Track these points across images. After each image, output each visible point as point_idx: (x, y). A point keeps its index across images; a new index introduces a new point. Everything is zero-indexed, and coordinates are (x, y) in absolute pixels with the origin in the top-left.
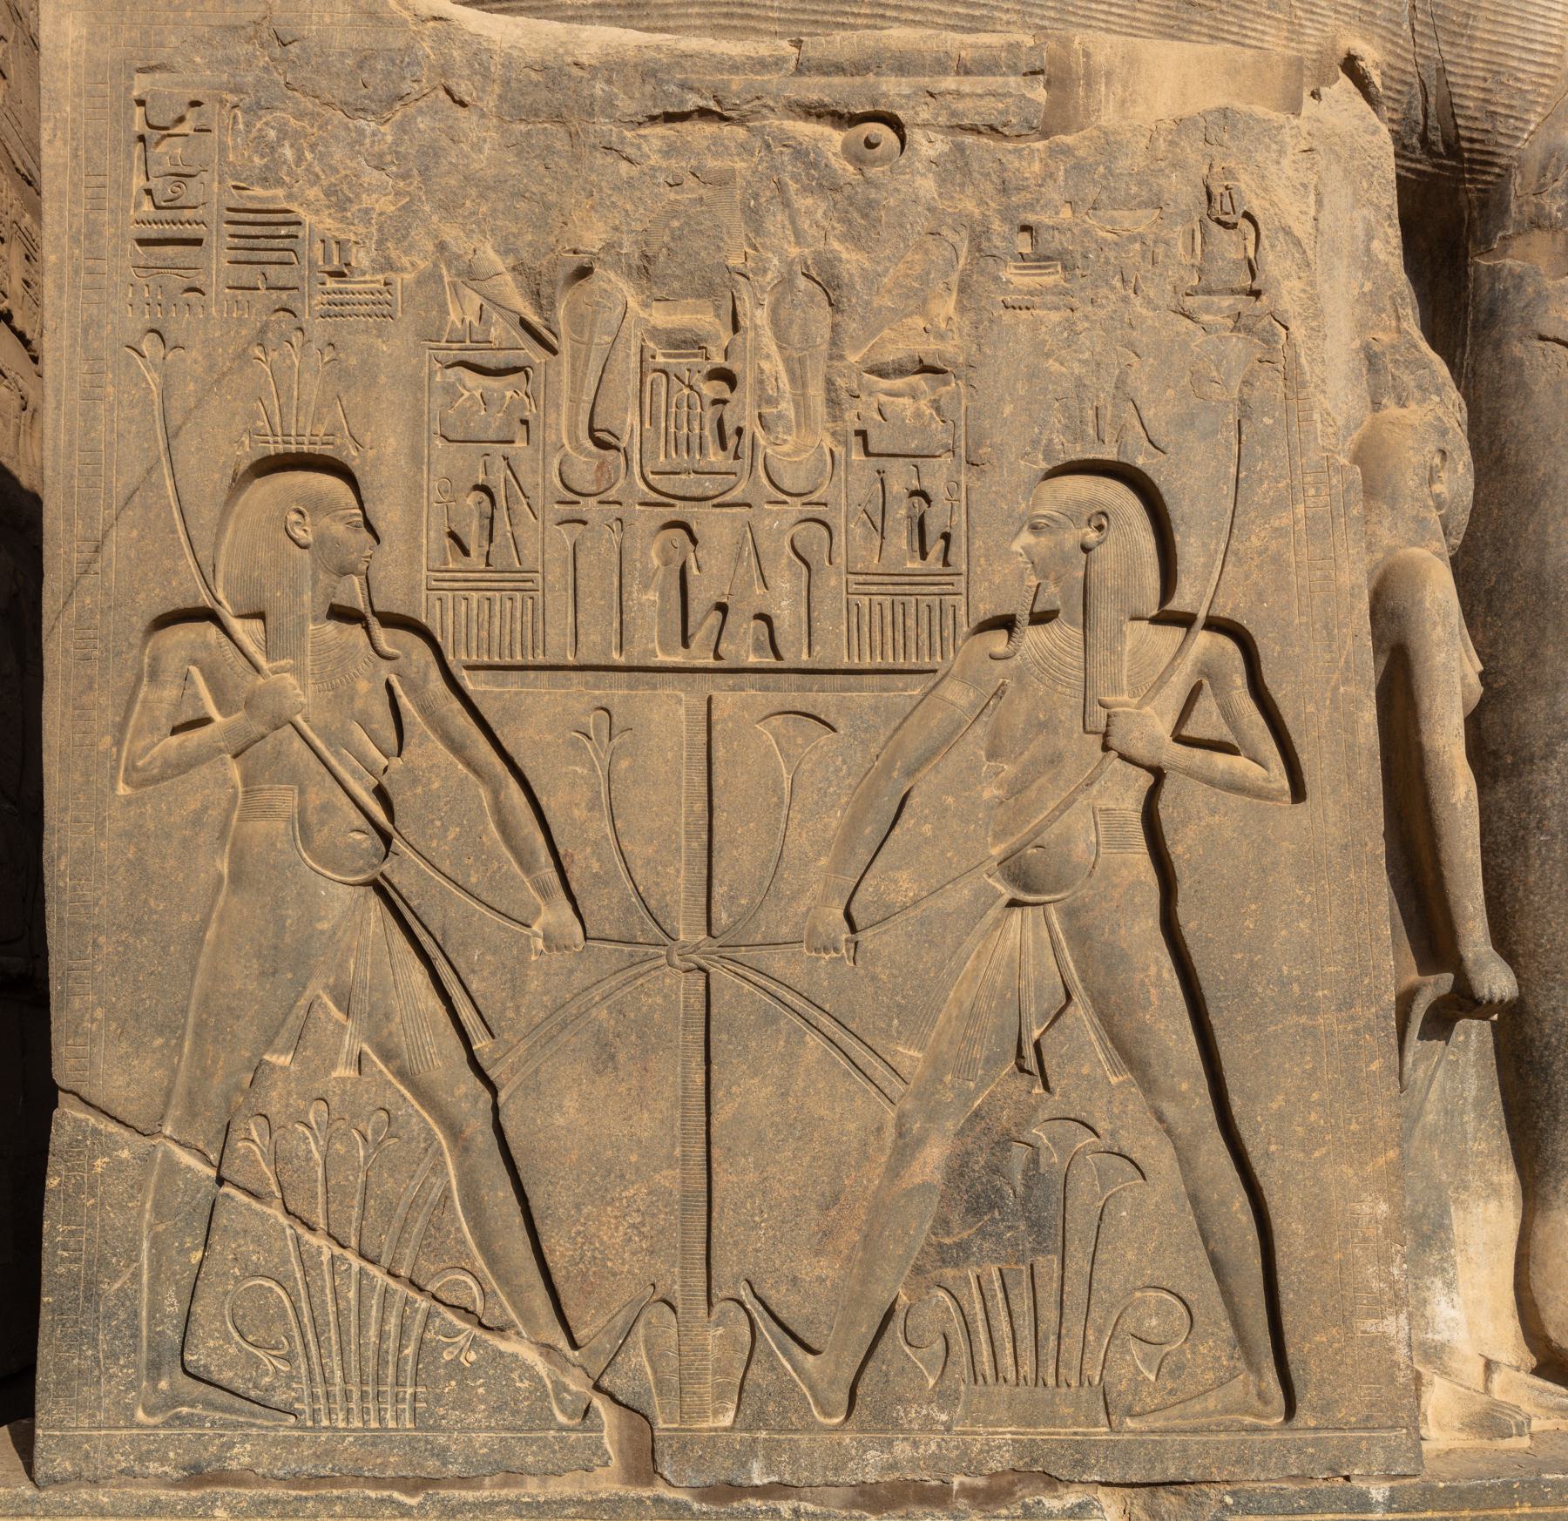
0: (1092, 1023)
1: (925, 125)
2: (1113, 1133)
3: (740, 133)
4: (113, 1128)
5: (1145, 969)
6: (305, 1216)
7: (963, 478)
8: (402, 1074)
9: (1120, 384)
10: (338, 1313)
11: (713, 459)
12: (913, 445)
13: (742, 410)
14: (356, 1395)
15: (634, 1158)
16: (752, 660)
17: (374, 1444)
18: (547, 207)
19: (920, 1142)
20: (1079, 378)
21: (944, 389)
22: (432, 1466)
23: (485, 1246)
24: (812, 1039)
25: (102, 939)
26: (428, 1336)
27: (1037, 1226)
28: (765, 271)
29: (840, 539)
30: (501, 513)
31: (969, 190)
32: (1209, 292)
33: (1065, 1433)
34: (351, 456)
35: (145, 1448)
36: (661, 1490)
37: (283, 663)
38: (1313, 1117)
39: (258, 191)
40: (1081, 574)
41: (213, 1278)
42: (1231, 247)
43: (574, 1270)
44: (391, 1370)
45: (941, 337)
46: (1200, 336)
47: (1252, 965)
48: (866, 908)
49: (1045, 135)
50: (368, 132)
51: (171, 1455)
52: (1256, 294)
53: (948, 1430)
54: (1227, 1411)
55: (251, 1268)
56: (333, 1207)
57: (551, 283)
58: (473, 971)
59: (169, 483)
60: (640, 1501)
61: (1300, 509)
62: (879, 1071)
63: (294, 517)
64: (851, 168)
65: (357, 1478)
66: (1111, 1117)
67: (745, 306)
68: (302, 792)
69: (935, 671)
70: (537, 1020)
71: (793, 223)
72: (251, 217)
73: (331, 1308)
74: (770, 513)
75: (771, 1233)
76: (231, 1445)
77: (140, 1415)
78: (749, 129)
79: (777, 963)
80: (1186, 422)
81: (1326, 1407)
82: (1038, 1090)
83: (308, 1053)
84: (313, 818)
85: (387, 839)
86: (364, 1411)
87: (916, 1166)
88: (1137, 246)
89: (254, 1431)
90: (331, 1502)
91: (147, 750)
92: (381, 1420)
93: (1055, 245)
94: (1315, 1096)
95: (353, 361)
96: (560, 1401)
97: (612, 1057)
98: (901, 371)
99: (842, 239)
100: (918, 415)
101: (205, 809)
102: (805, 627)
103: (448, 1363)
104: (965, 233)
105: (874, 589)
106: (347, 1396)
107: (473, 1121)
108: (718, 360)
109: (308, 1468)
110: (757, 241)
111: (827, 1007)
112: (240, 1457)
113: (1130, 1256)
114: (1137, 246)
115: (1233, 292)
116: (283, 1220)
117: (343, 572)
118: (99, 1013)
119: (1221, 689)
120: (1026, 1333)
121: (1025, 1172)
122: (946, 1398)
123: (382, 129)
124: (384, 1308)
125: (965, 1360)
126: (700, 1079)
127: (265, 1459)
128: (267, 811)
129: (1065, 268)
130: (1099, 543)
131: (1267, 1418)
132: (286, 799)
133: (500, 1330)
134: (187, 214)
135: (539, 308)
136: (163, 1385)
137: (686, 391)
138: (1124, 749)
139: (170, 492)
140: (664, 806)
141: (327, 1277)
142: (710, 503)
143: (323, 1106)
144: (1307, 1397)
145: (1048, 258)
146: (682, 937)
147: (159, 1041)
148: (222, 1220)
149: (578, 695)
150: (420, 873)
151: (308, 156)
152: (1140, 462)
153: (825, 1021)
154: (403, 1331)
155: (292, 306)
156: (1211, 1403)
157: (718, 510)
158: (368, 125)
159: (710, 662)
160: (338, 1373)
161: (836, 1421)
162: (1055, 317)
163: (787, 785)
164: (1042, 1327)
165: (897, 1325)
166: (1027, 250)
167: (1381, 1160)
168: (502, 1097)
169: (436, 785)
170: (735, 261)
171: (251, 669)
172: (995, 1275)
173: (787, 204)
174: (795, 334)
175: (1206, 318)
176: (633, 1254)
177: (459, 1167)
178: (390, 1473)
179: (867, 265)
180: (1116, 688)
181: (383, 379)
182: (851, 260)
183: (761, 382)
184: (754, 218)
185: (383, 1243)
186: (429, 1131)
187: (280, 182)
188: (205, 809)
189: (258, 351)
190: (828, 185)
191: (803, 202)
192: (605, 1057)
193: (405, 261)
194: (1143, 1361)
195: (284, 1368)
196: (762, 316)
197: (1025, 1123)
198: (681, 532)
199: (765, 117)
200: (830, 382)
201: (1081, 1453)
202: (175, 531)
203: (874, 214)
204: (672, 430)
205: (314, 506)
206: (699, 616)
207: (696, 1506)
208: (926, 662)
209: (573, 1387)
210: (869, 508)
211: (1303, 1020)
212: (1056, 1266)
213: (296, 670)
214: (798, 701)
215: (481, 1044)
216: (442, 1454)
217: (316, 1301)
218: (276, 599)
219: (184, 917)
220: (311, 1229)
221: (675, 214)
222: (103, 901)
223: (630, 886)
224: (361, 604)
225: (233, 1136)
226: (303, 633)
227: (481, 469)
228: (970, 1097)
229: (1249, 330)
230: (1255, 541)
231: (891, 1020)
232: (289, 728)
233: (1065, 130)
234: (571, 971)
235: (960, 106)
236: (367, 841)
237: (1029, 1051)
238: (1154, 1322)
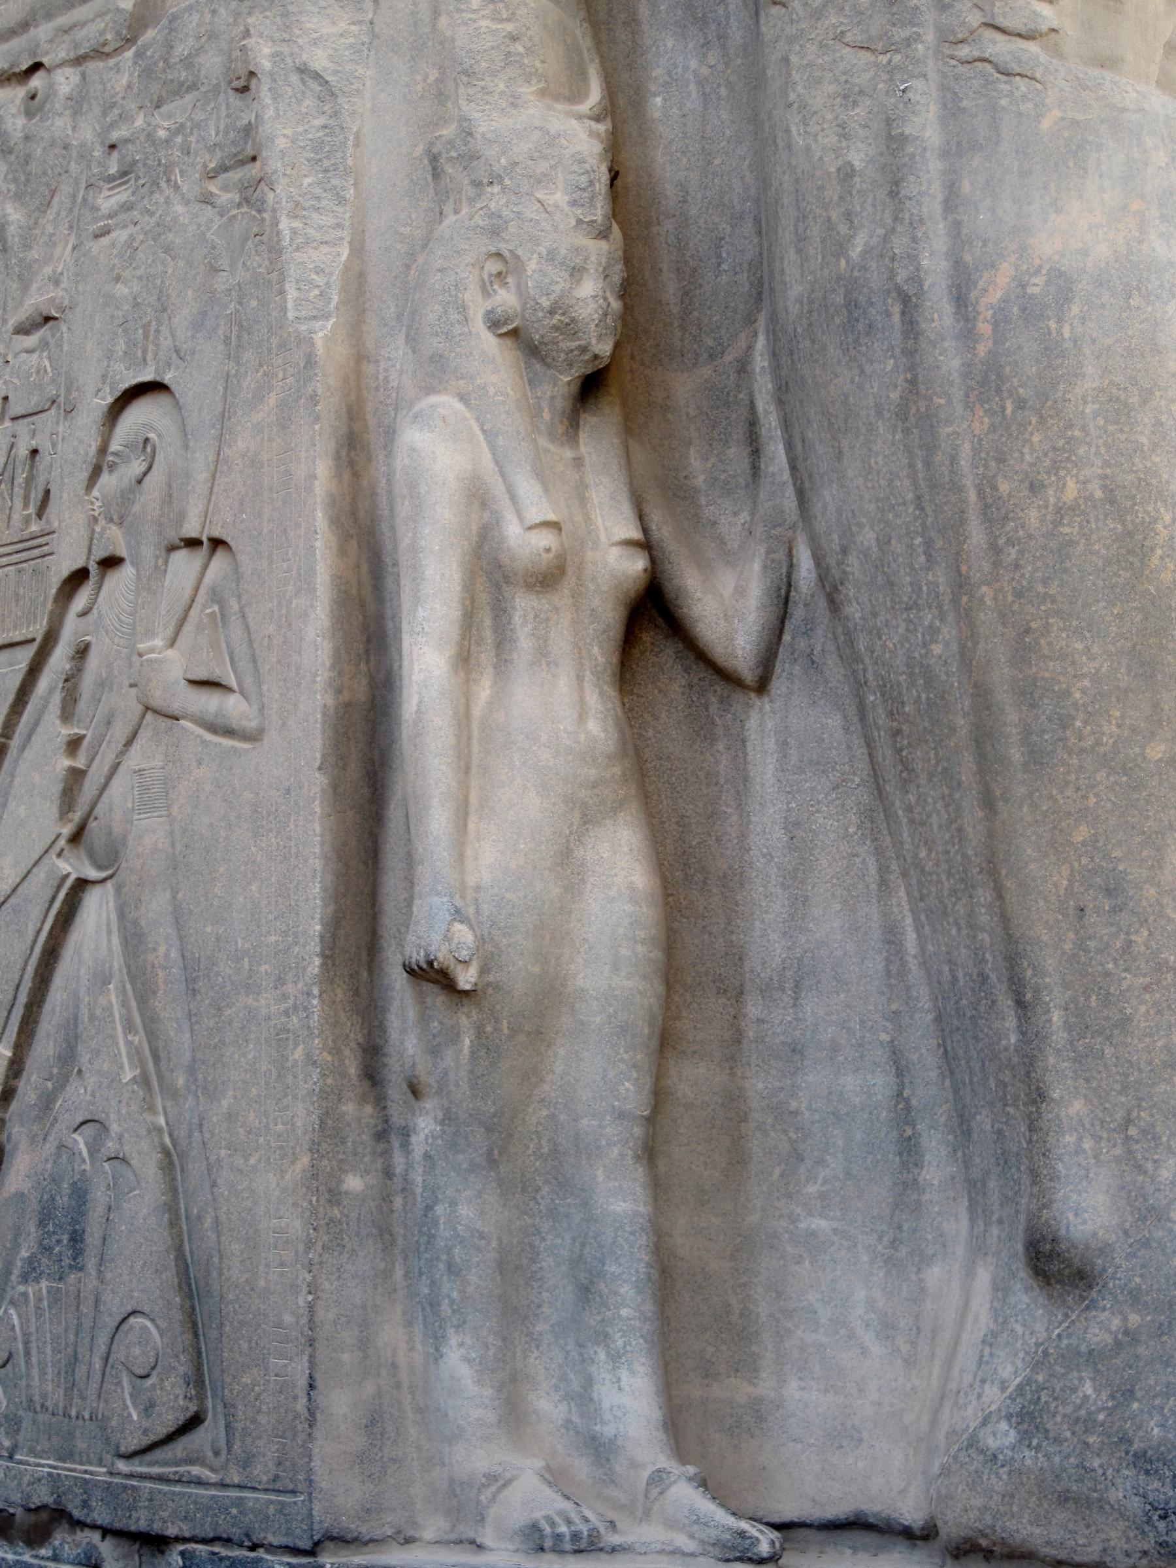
5: (154, 950)
61: (272, 400)
69: (33, 640)
81: (246, 1462)
115: (242, 163)
194: (131, 1395)
230: (241, 444)
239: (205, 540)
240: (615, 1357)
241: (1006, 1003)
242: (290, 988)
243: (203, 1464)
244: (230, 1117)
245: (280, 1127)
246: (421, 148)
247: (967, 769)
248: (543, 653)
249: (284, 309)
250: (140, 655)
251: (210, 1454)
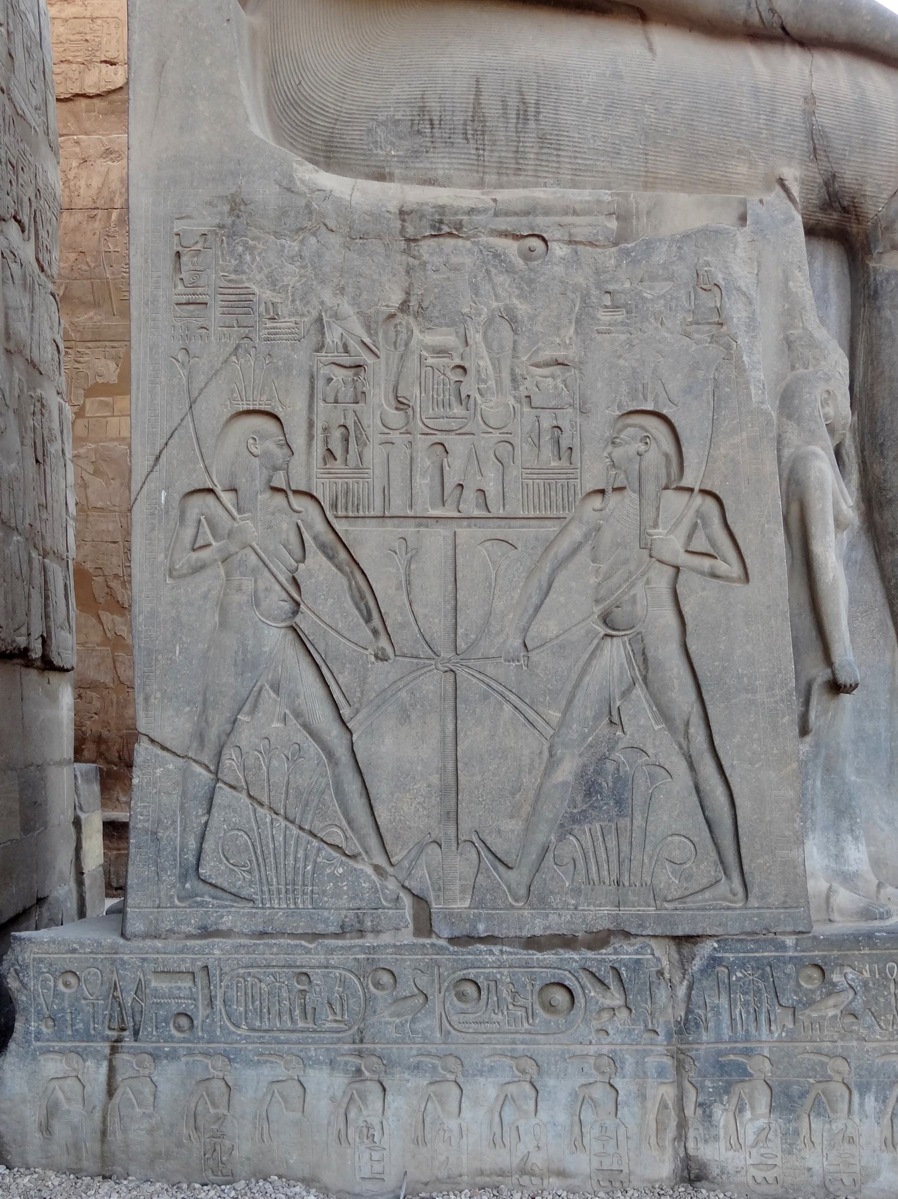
0: (645, 698)
1: (557, 241)
2: (656, 755)
3: (468, 244)
4: (165, 753)
6: (259, 798)
7: (578, 420)
8: (306, 726)
9: (655, 371)
10: (274, 849)
11: (455, 411)
12: (553, 403)
13: (469, 387)
14: (283, 891)
15: (419, 768)
16: (476, 513)
17: (293, 916)
18: (373, 281)
19: (561, 760)
20: (633, 368)
21: (568, 374)
22: (321, 928)
23: (346, 814)
24: (507, 707)
25: (160, 657)
26: (319, 860)
27: (619, 803)
28: (480, 315)
29: (518, 452)
30: (352, 439)
31: (580, 272)
32: (698, 324)
33: (633, 910)
34: (279, 411)
35: (179, 918)
36: (434, 940)
37: (246, 515)
38: (755, 746)
39: (233, 276)
40: (637, 467)
41: (214, 830)
42: (710, 301)
43: (390, 826)
44: (300, 877)
45: (567, 347)
46: (694, 347)
47: (724, 668)
48: (533, 639)
49: (616, 244)
50: (287, 246)
51: (193, 921)
52: (722, 324)
53: (576, 909)
54: (715, 899)
55: (232, 825)
56: (272, 794)
57: (376, 322)
58: (340, 673)
59: (191, 425)
60: (424, 945)
61: (744, 434)
62: (540, 723)
63: (251, 441)
64: (521, 262)
65: (283, 934)
66: (655, 746)
67: (471, 333)
68: (256, 581)
70: (371, 698)
71: (493, 288)
72: (231, 291)
73: (271, 846)
74: (483, 438)
75: (487, 806)
76: (222, 917)
77: (177, 902)
78: (473, 243)
79: (490, 670)
80: (688, 390)
81: (763, 896)
82: (619, 733)
83: (260, 715)
84: (261, 595)
85: (298, 604)
86: (287, 899)
87: (559, 772)
88: (662, 301)
89: (233, 909)
90: (271, 946)
91: (180, 560)
92: (295, 903)
93: (622, 301)
94: (756, 736)
95: (280, 363)
96: (384, 894)
97: (408, 717)
98: (547, 365)
99: (519, 297)
100: (556, 387)
101: (209, 591)
102: (501, 496)
103: (328, 874)
104: (578, 294)
105: (535, 476)
106: (279, 892)
107: (340, 749)
108: (458, 361)
109: (261, 928)
110: (476, 300)
111: (514, 691)
112: (227, 922)
113: (665, 818)
114: (662, 301)
115: (710, 323)
116: (248, 801)
117: (276, 469)
118: (158, 695)
119: (705, 525)
120: (614, 858)
121: (613, 775)
122: (576, 891)
123: (293, 244)
124: (297, 846)
125: (584, 872)
126: (451, 727)
127: (239, 924)
128: (239, 589)
129: (627, 312)
130: (646, 452)
131: (735, 902)
132: (248, 584)
133: (353, 857)
134: (200, 290)
135: (370, 335)
136: (188, 885)
137: (442, 377)
138: (659, 557)
139: (192, 430)
140: (432, 591)
141: (269, 829)
142: (454, 433)
143: (266, 741)
144: (755, 891)
145: (618, 307)
146: (442, 655)
147: (187, 709)
148: (217, 800)
149: (391, 530)
150: (314, 622)
151: (258, 258)
152: (665, 411)
153: (513, 697)
154: (306, 858)
155: (251, 336)
156: (707, 894)
157: (458, 437)
158: (287, 242)
159: (457, 515)
160: (275, 879)
161: (521, 904)
162: (623, 337)
163: (493, 576)
164: (622, 855)
165: (550, 855)
166: (609, 303)
167: (789, 768)
168: (354, 738)
169: (321, 578)
170: (466, 310)
171: (230, 518)
172: (598, 828)
173: (491, 280)
174: (495, 346)
175: (696, 336)
176: (419, 818)
177: (333, 772)
178: (300, 931)
179: (529, 311)
180: (655, 526)
181: (294, 372)
182: (522, 308)
183: (479, 371)
184: (476, 289)
185: (295, 812)
186: (319, 754)
187: (244, 272)
188: (209, 591)
189: (234, 358)
190: (510, 270)
192: (404, 716)
193: (305, 310)
194: (672, 873)
195: (248, 877)
196: (479, 337)
197: (611, 749)
198: (440, 447)
199: (479, 236)
200: (512, 370)
201: (642, 919)
202: (194, 450)
203: (533, 286)
204: (435, 396)
206: (449, 491)
207: (451, 948)
208: (561, 514)
209: (390, 887)
210: (533, 435)
211: (750, 696)
212: (629, 824)
213: (253, 519)
214: (499, 533)
215: (345, 711)
216: (325, 921)
217: (264, 842)
218: (242, 482)
219: (200, 646)
220: (261, 804)
221: (436, 286)
222: (160, 638)
223: (417, 628)
224: (285, 488)
225: (223, 757)
226: (256, 500)
227: (342, 417)
228: (585, 737)
229: (716, 342)
230: (722, 451)
231: (546, 696)
232: (248, 550)
233: (626, 241)
234: (388, 673)
235: (574, 231)
236: (287, 606)
237: (615, 712)
238: (677, 852)
239: (697, 489)
242: (777, 691)
243: (725, 899)
245: (775, 751)
246: (782, 336)
249: (749, 395)
250: (650, 535)
251: (730, 896)
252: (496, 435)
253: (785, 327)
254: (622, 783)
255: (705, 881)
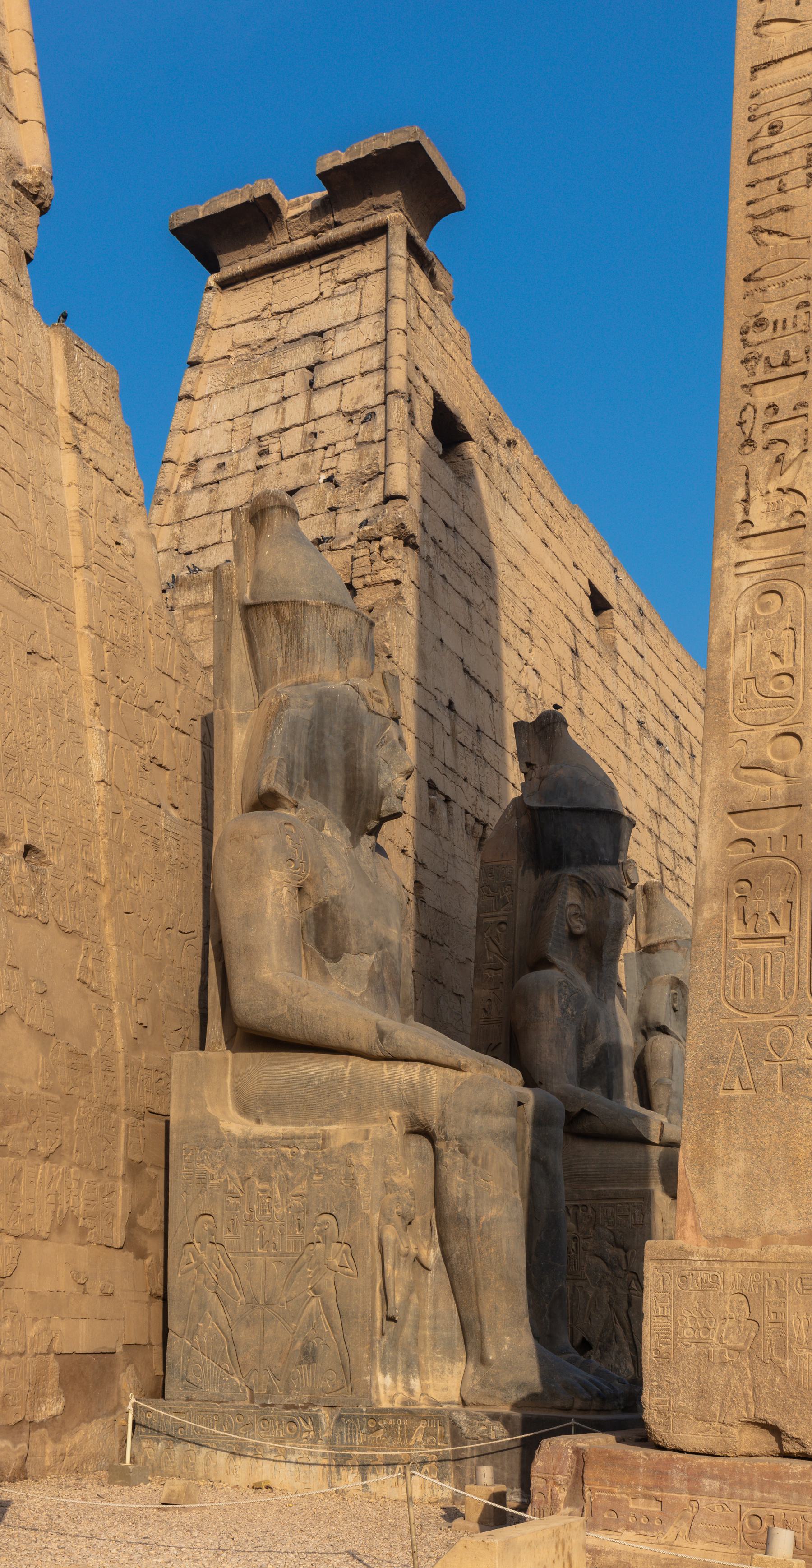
22: (222, 1399)
34: (213, 1214)
98: (297, 1196)
132: (203, 1277)
133: (232, 1374)
156: (340, 1392)
182: (290, 1174)
191: (283, 1164)
201: (318, 1400)
205: (208, 1222)
240: (414, 1377)
241: (478, 1324)
244: (352, 1338)
247: (473, 1289)
248: (405, 1266)
252: (280, 1222)
253: (384, 1178)
254: (314, 1350)
255: (339, 1387)
